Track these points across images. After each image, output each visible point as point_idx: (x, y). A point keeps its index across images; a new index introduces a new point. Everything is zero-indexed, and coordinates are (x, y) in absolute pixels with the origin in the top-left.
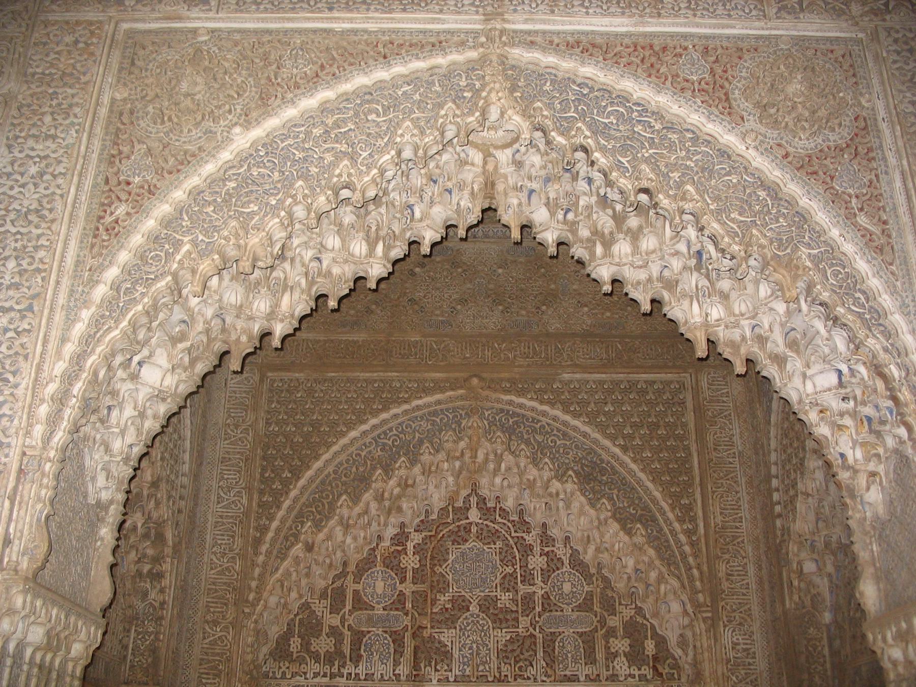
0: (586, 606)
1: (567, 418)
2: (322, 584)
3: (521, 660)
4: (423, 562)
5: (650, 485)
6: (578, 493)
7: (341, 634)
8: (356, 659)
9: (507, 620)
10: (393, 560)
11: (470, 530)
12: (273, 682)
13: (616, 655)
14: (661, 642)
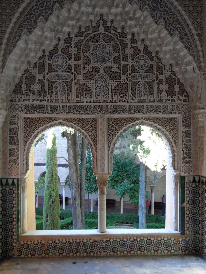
0: (150, 70)
3: (121, 93)
5: (183, 12)
6: (150, 17)
8: (51, 94)
9: (116, 77)
11: (100, 37)
12: (15, 103)
14: (182, 86)
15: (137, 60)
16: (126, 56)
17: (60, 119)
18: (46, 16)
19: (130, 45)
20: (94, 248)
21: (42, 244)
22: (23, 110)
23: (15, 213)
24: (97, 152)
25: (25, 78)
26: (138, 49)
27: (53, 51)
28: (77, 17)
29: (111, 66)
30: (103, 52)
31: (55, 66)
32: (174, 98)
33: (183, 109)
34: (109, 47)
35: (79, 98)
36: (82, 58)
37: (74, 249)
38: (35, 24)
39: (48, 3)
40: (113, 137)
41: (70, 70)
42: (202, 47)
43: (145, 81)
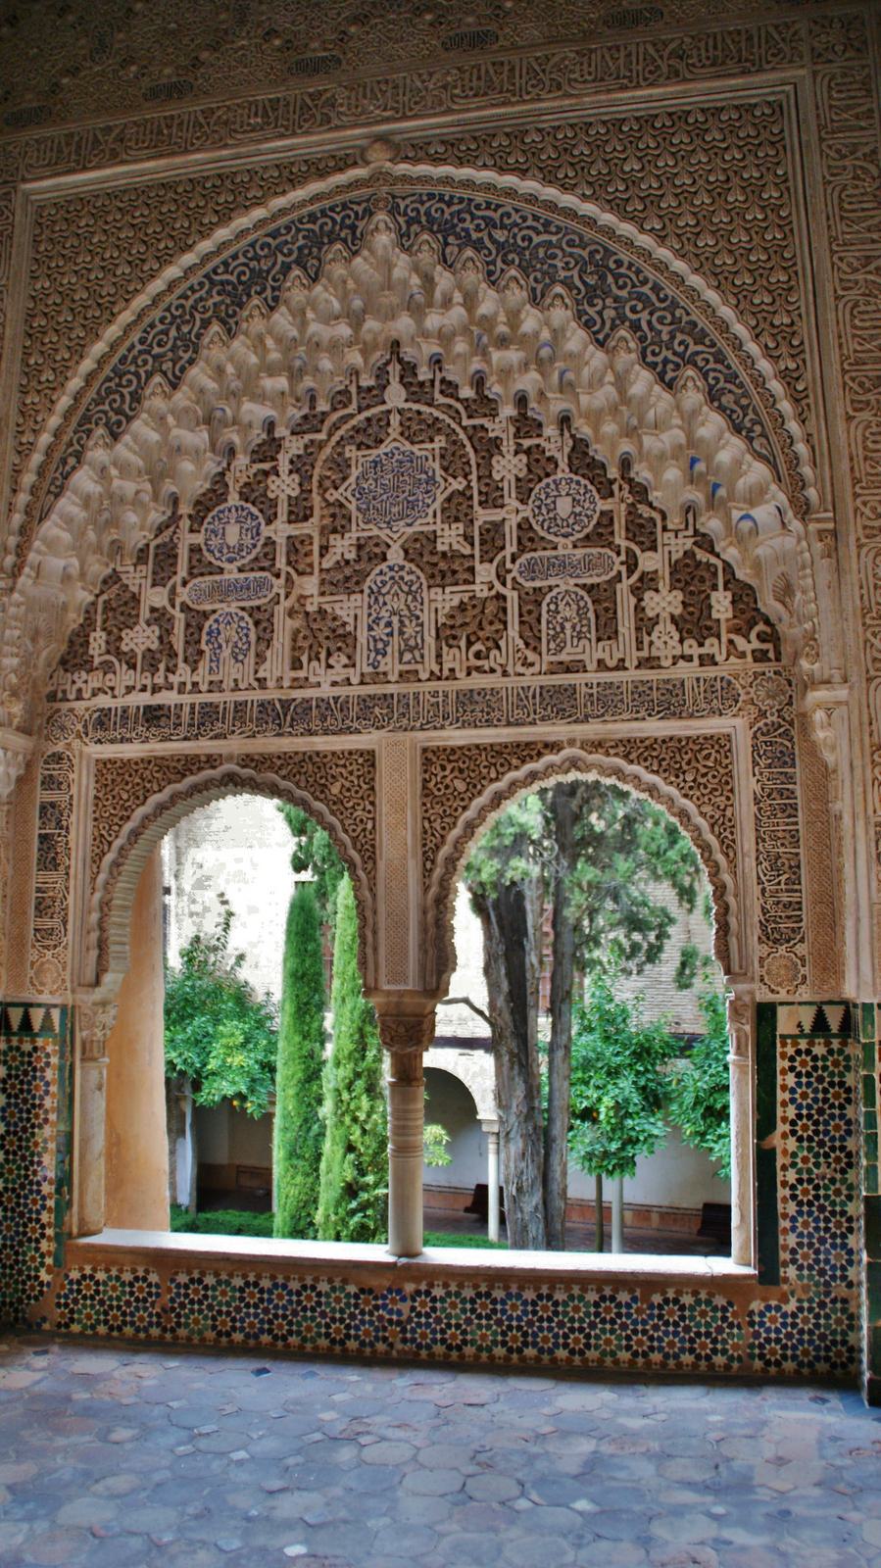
0: (601, 534)
1: (550, 193)
2: (137, 538)
3: (479, 639)
4: (306, 486)
5: (712, 296)
6: (573, 324)
7: (171, 619)
9: (454, 572)
11: (388, 424)
12: (65, 706)
13: (655, 621)
14: (744, 596)
15: (543, 497)
17: (230, 758)
18: (174, 373)
19: (511, 443)
20: (363, 1322)
21: (150, 1285)
22: (90, 728)
23: (52, 1146)
24: (374, 896)
25: (105, 610)
26: (548, 454)
28: (298, 363)
29: (435, 532)
31: (212, 552)
32: (711, 646)
33: (752, 695)
35: (301, 668)
36: (317, 512)
37: (276, 1316)
40: (443, 828)
42: (803, 422)
43: (581, 581)
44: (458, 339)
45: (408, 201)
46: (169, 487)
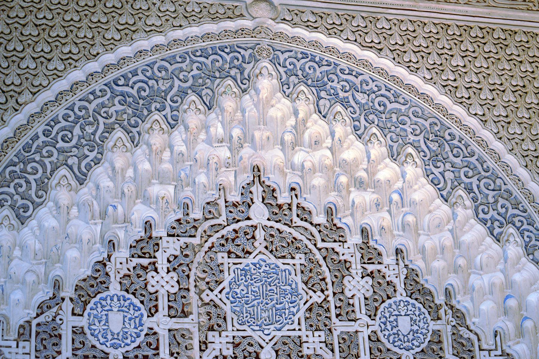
6: (423, 180)
10: (134, 279)
11: (253, 237)
15: (387, 315)
16: (349, 304)
18: (79, 168)
19: (359, 267)
26: (388, 279)
27: (93, 282)
29: (300, 337)
30: (269, 288)
31: (96, 336)
34: (290, 274)
36: (195, 309)
38: (40, 193)
39: (87, 128)
41: (154, 352)
44: (317, 174)
45: (287, 55)
46: (57, 271)
